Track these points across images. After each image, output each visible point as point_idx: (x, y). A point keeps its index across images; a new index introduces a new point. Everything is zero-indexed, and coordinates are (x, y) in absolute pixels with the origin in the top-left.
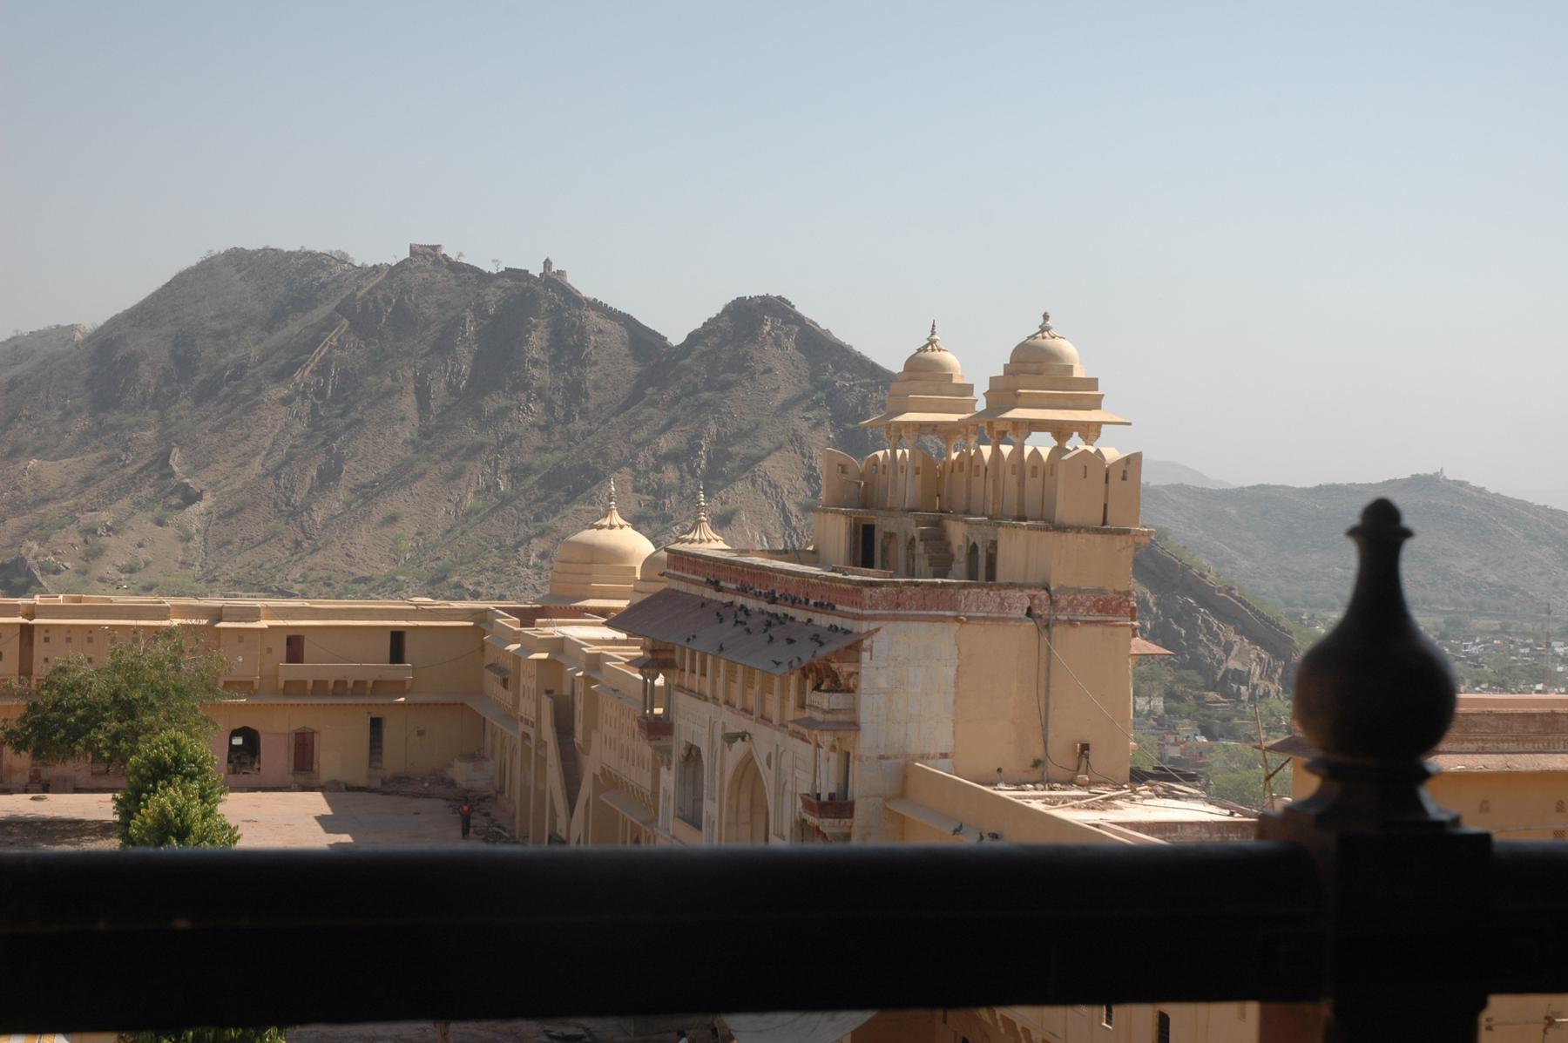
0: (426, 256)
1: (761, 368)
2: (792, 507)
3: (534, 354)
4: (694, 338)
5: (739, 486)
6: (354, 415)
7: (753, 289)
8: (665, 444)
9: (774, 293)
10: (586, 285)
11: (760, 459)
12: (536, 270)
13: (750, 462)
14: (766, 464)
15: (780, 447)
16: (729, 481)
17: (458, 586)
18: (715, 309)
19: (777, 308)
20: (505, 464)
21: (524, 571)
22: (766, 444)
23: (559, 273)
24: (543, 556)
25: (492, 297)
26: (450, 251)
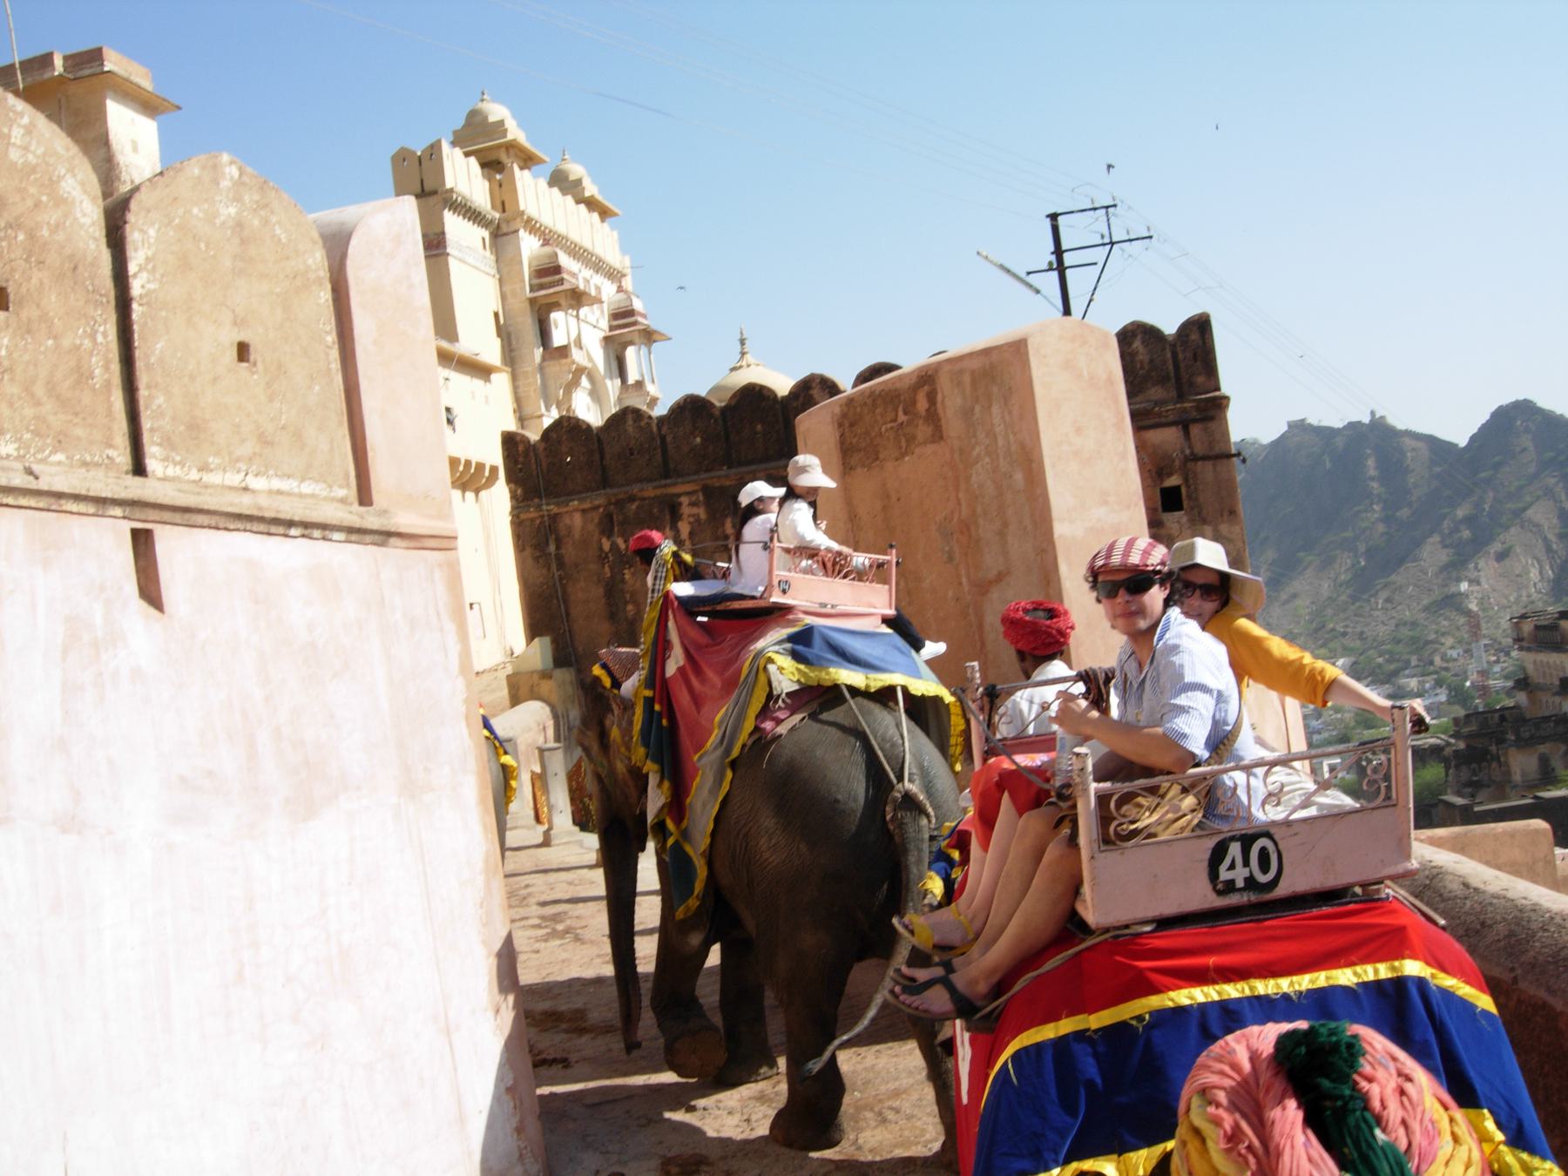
0: (1298, 428)
1: (1518, 449)
2: (1551, 536)
3: (1372, 472)
4: (1473, 439)
5: (1513, 530)
6: (1262, 535)
7: (1506, 399)
8: (1461, 513)
9: (1521, 398)
10: (1402, 419)
11: (1524, 510)
12: (1366, 420)
13: (1518, 513)
14: (1529, 512)
15: (1538, 498)
16: (1506, 528)
17: (1333, 630)
18: (1484, 417)
19: (1524, 409)
20: (1362, 548)
21: (1376, 613)
22: (1528, 499)
23: (1382, 418)
24: (1388, 600)
25: (1339, 442)
26: (1313, 420)
